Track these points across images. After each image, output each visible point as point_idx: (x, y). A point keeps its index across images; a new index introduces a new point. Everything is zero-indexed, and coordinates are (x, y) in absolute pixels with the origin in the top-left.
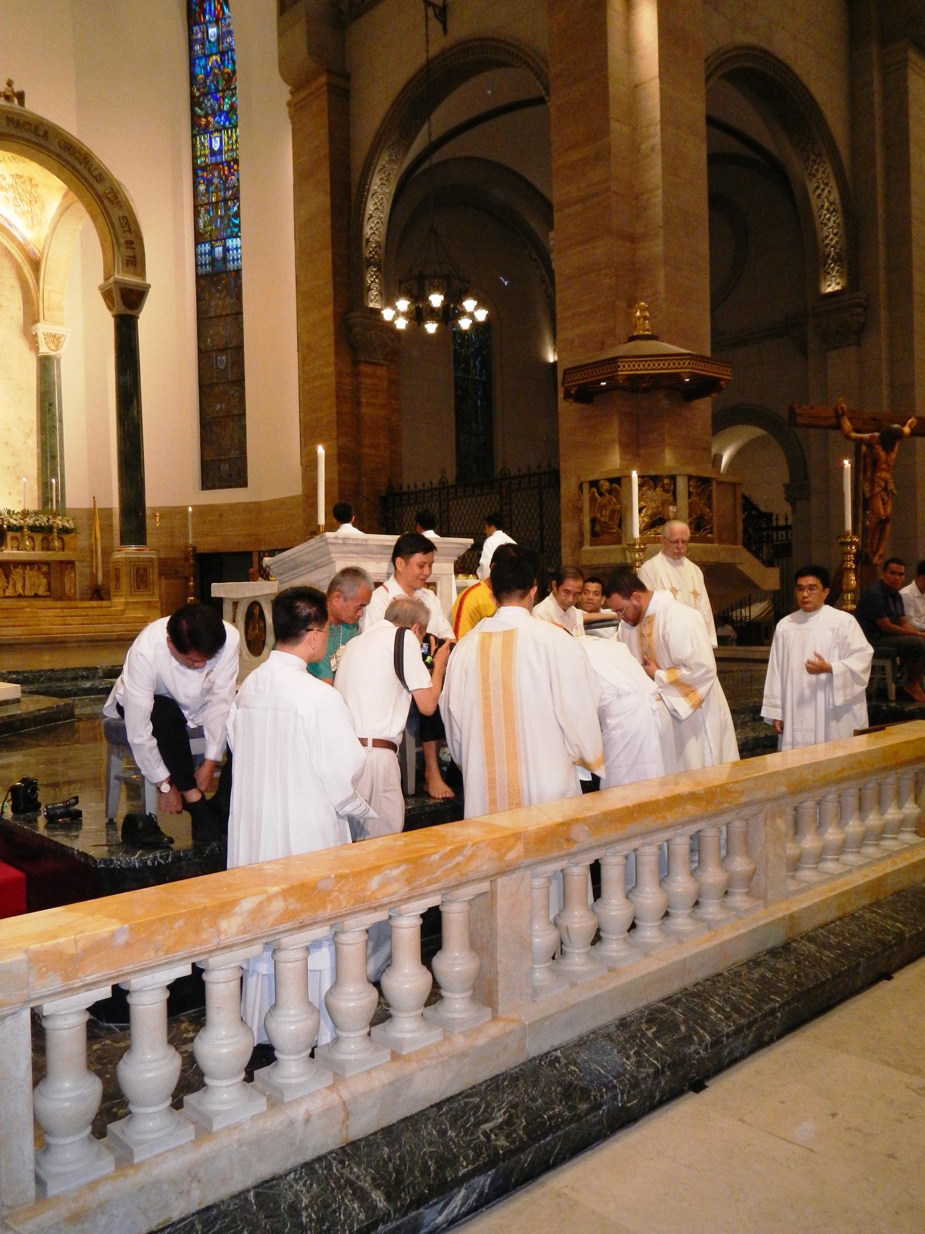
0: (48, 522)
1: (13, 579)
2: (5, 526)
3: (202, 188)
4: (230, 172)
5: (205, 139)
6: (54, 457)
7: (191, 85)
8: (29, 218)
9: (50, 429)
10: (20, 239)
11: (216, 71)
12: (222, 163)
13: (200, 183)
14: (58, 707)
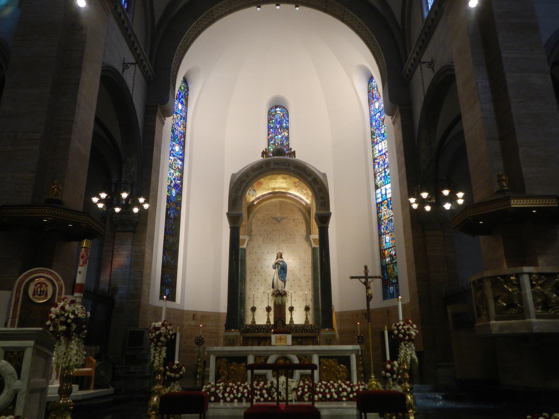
3: (377, 166)
4: (386, 157)
5: (376, 147)
7: (371, 127)
8: (307, 195)
10: (304, 204)
11: (379, 119)
12: (383, 154)
13: (375, 165)
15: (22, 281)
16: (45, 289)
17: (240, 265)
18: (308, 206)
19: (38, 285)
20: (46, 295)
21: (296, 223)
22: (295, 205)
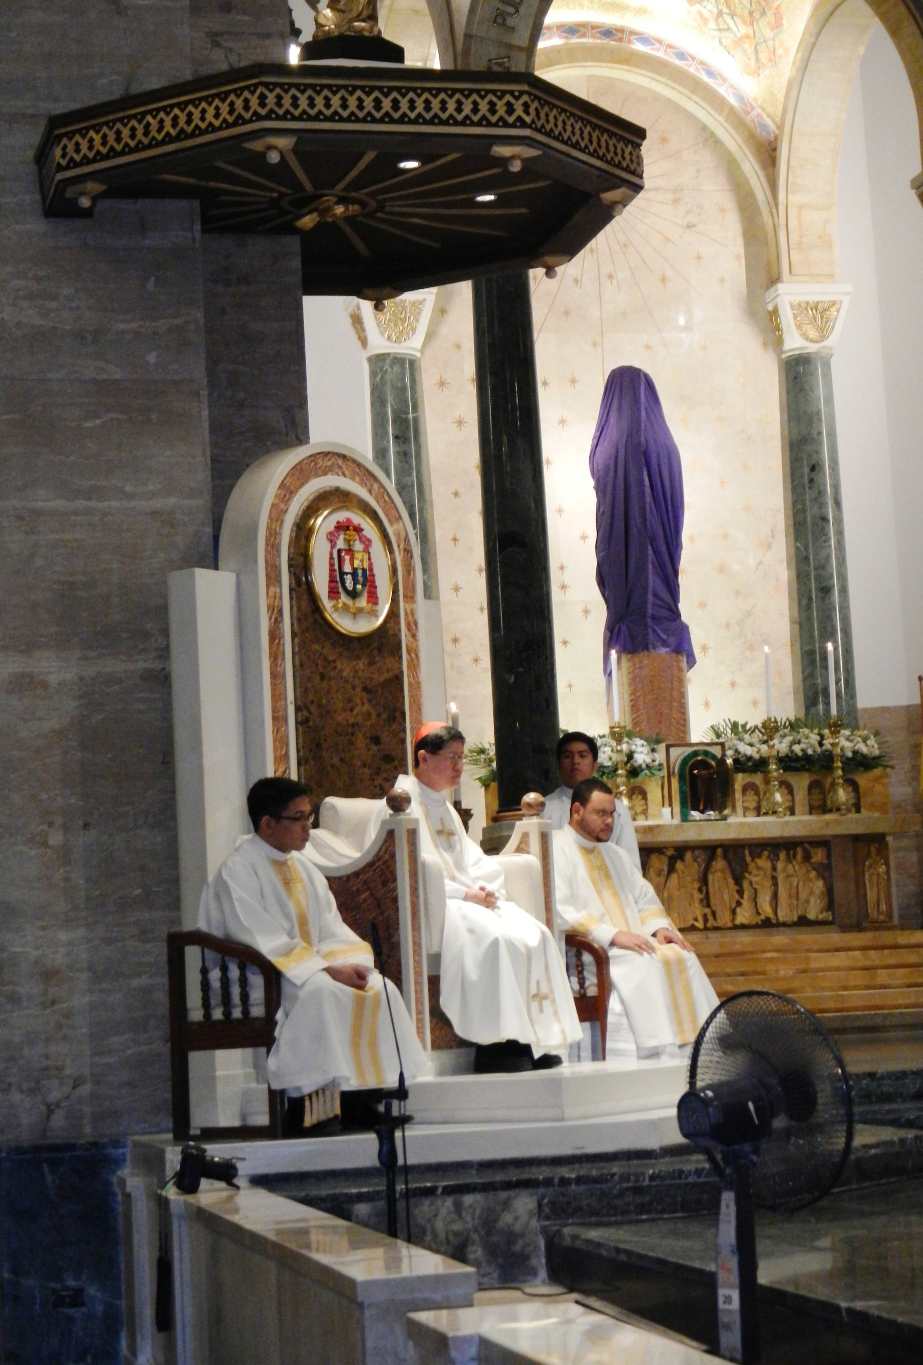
0: (821, 744)
1: (751, 883)
2: (729, 761)
6: (826, 590)
8: (750, 50)
9: (814, 524)
10: (732, 100)
14: (902, 1141)
15: (277, 515)
16: (366, 566)
17: (397, 453)
18: (753, 114)
19: (337, 538)
20: (373, 598)
21: (688, 212)
22: (677, 108)
